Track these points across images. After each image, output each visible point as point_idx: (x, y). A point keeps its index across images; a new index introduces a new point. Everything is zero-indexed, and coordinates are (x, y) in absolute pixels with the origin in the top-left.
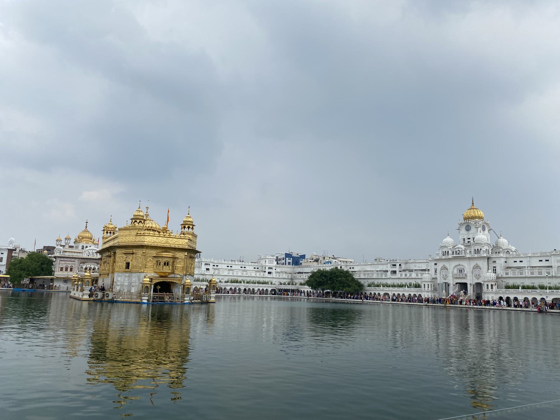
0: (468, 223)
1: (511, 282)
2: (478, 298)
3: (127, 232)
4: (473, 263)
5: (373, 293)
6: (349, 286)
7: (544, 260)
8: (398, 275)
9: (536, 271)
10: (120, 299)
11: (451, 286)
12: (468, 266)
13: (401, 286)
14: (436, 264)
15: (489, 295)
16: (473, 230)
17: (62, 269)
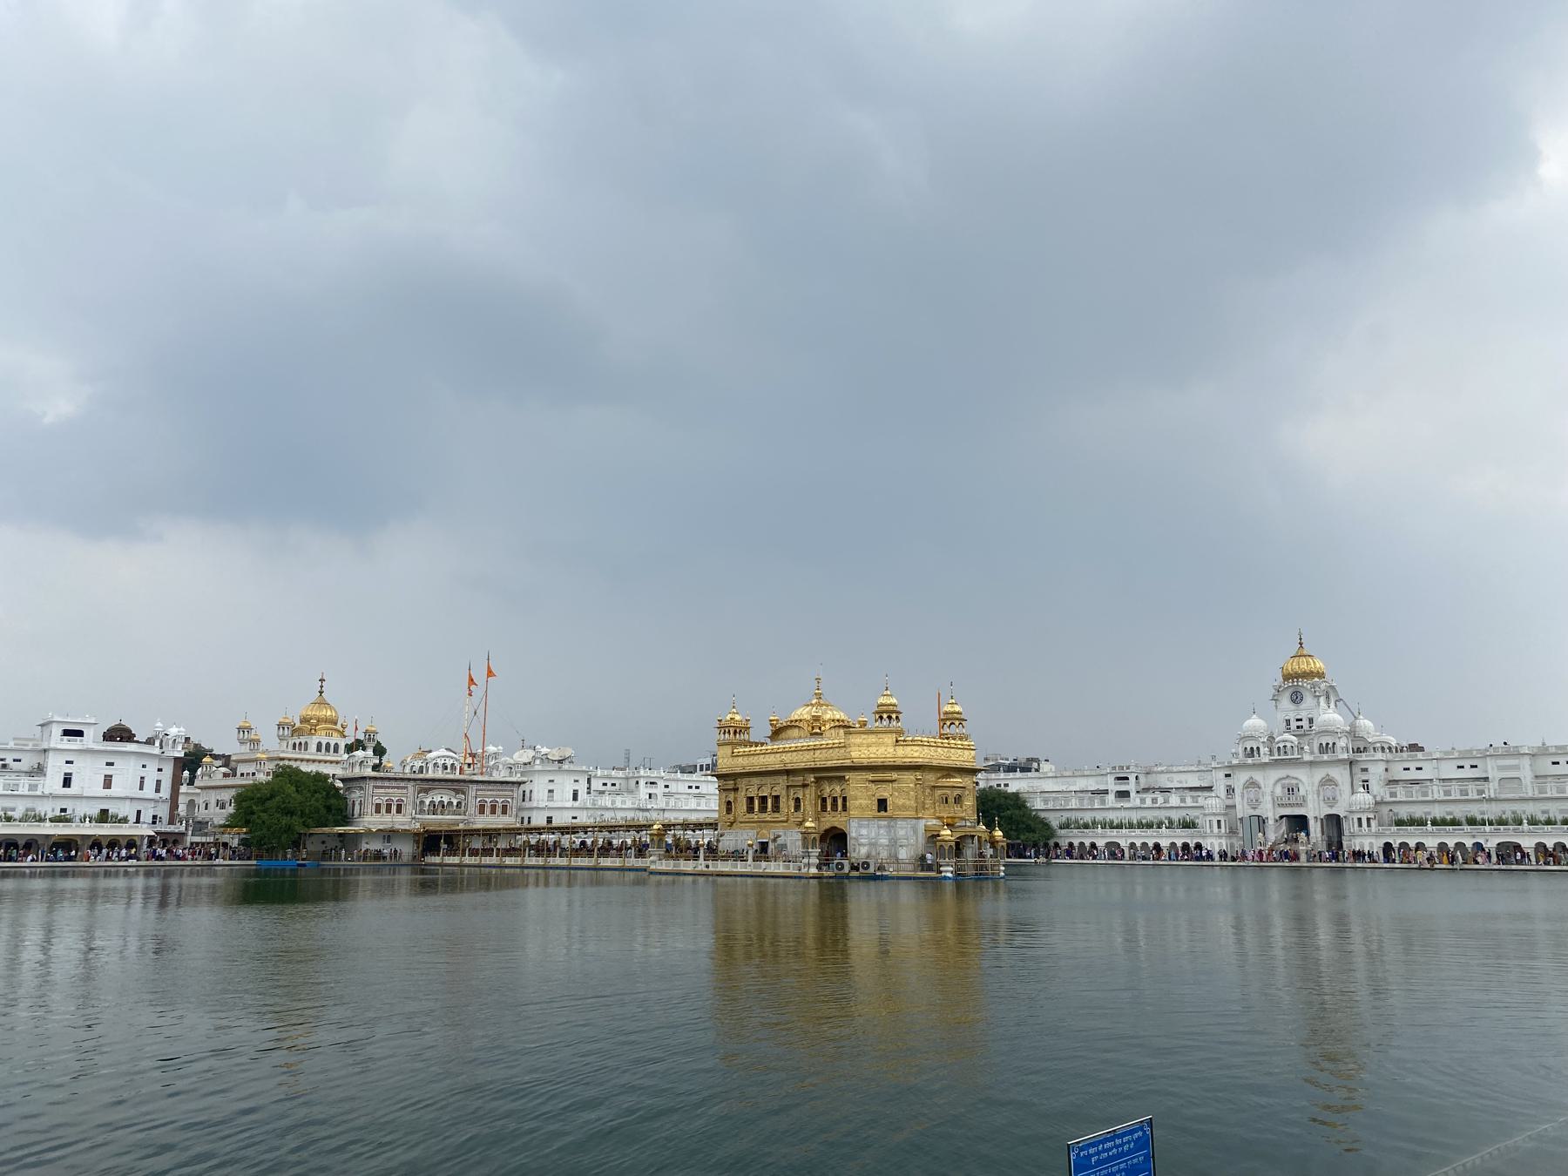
0: (1296, 683)
1: (1404, 812)
2: (1335, 846)
3: (872, 739)
4: (1320, 774)
5: (1076, 843)
6: (1030, 829)
7: (1467, 764)
8: (1135, 800)
10: (891, 871)
11: (1271, 822)
12: (1307, 781)
13: (1149, 826)
14: (1228, 776)
16: (1308, 701)
17: (378, 809)
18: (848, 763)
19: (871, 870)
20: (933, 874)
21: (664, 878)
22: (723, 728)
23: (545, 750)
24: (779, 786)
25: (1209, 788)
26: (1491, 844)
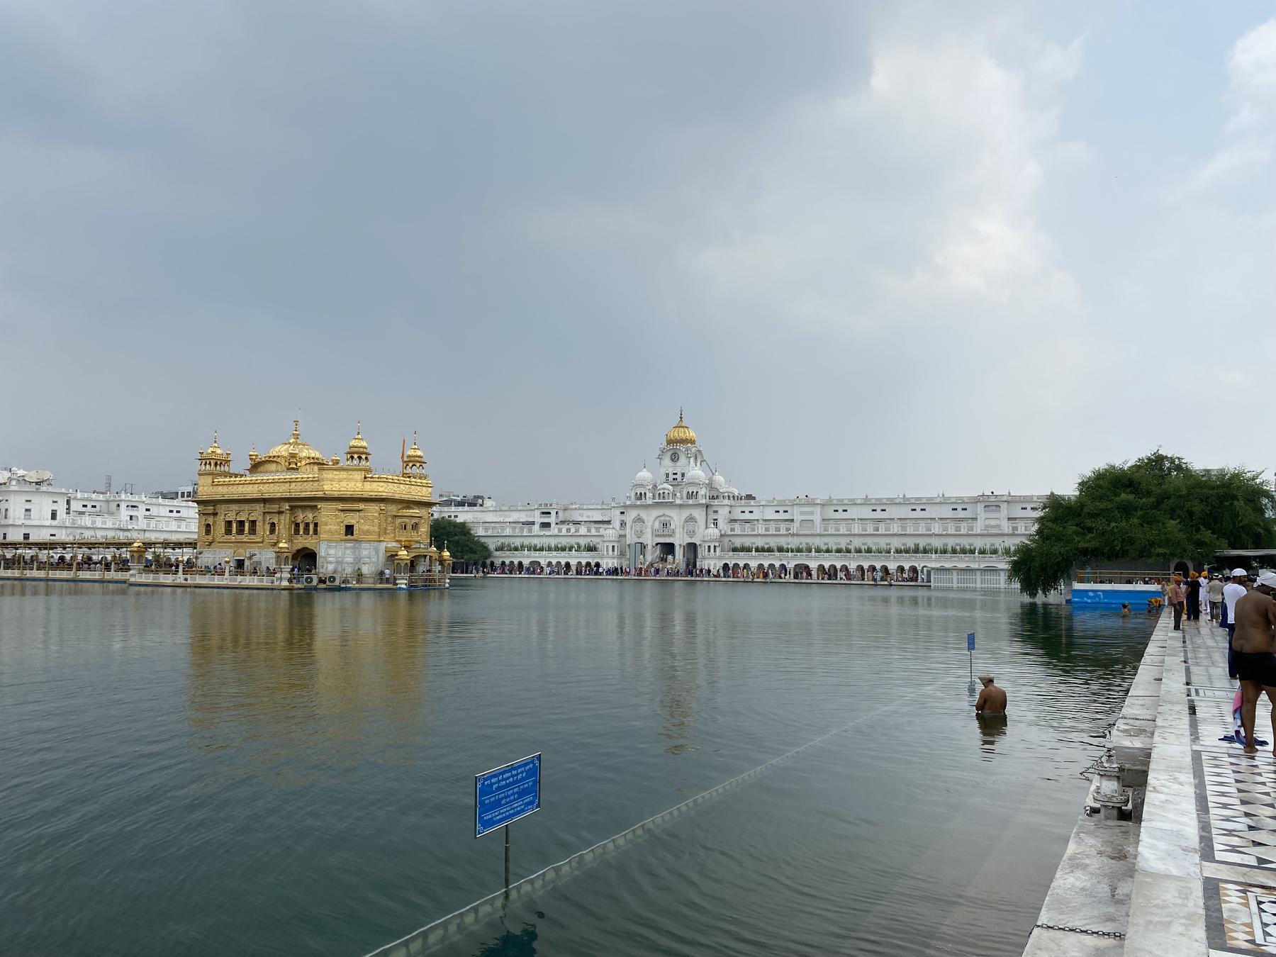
0: (676, 447)
1: (738, 542)
2: (691, 567)
3: (343, 475)
4: (686, 513)
5: (507, 562)
6: (472, 551)
8: (554, 530)
9: (772, 526)
11: (650, 547)
13: (563, 549)
15: (711, 562)
16: (683, 460)
18: (320, 494)
19: (337, 583)
20: (390, 586)
21: (143, 589)
22: (205, 460)
23: (21, 472)
24: (257, 513)
25: (609, 522)
26: (791, 565)
